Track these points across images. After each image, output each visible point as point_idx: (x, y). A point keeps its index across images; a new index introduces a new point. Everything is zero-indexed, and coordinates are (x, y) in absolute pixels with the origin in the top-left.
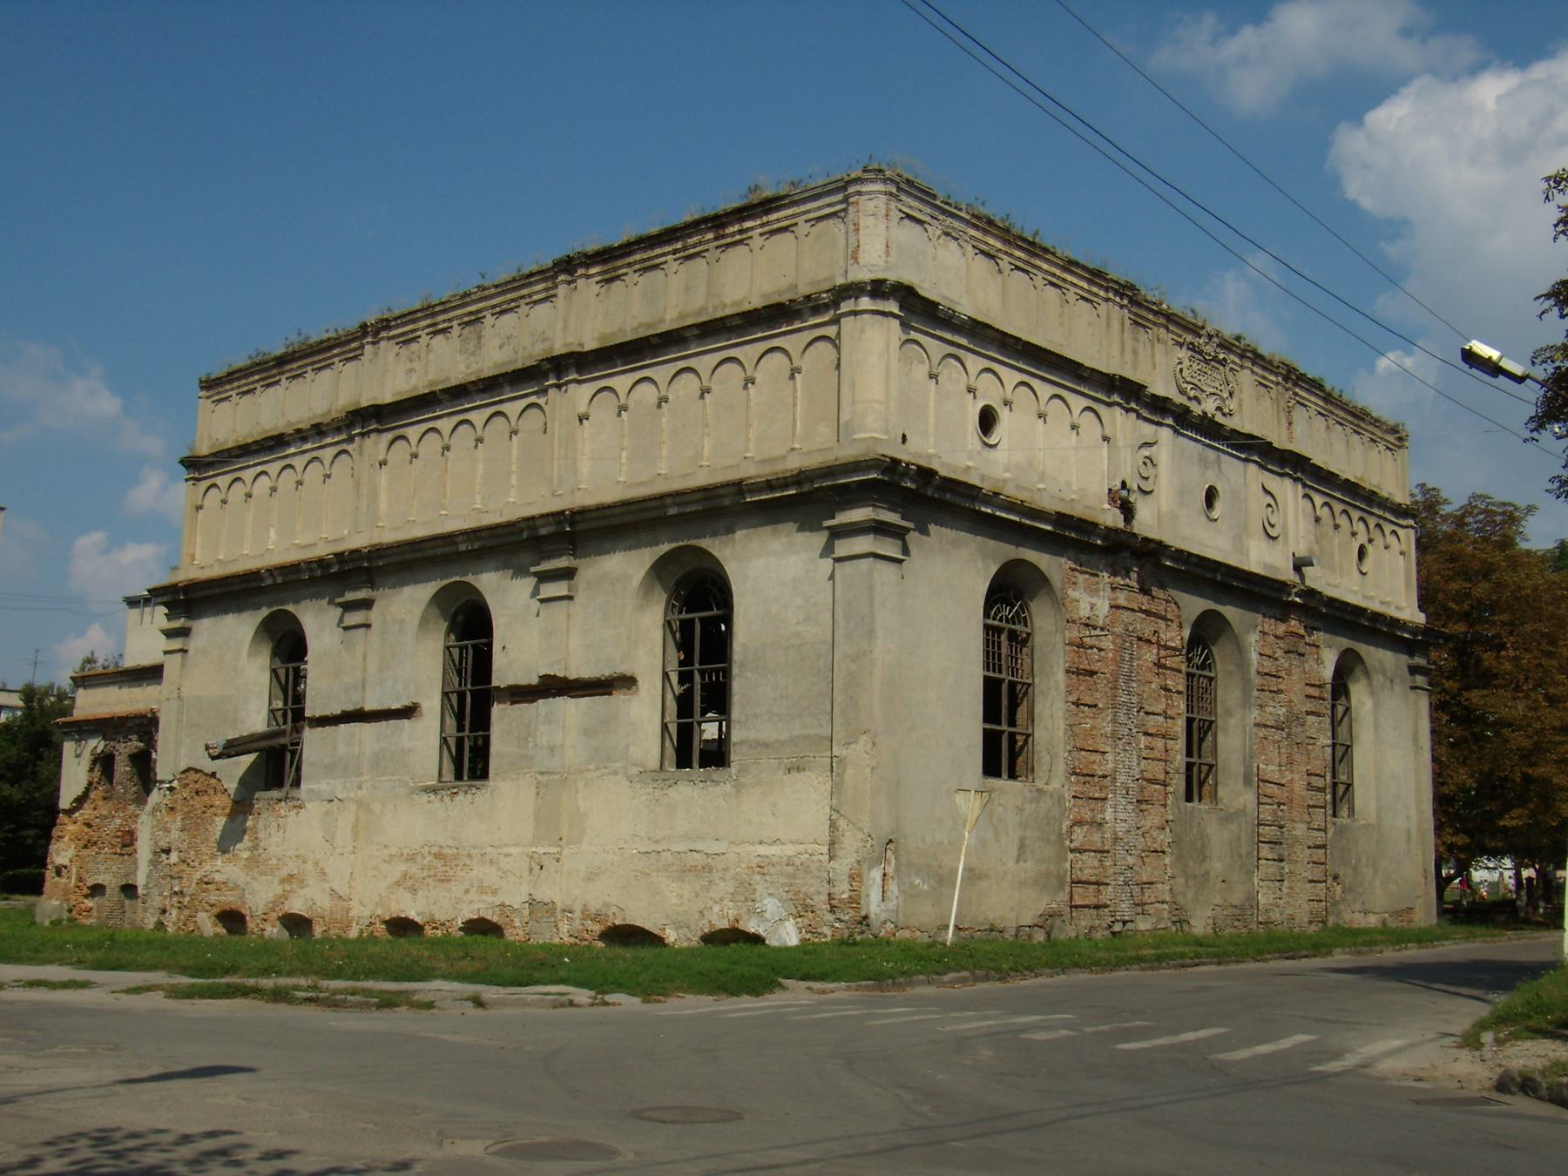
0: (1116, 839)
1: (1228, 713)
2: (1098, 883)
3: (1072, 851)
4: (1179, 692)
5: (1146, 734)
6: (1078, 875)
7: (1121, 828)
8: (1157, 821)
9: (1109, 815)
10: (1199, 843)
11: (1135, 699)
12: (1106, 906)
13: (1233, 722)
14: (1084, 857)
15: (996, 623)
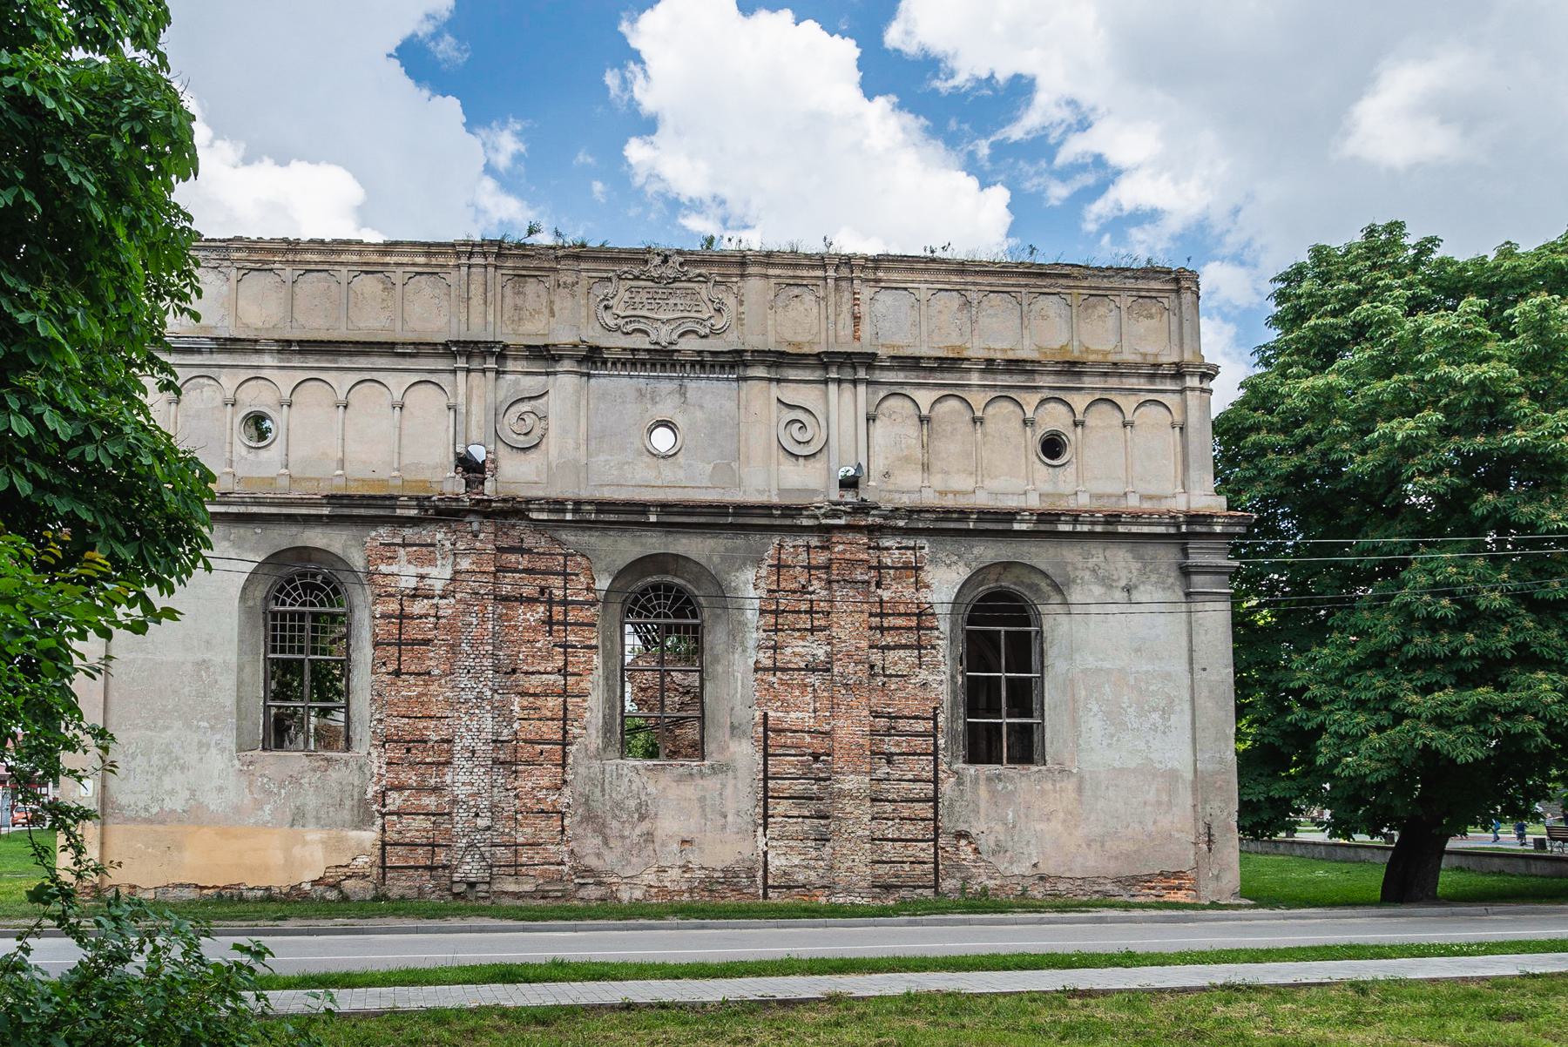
0: (454, 802)
1: (716, 660)
2: (434, 845)
3: (383, 815)
4: (590, 647)
5: (523, 694)
6: (392, 836)
7: (462, 792)
8: (545, 782)
9: (448, 779)
10: (632, 804)
11: (487, 662)
12: (444, 867)
13: (720, 669)
14: (406, 820)
15: (296, 608)
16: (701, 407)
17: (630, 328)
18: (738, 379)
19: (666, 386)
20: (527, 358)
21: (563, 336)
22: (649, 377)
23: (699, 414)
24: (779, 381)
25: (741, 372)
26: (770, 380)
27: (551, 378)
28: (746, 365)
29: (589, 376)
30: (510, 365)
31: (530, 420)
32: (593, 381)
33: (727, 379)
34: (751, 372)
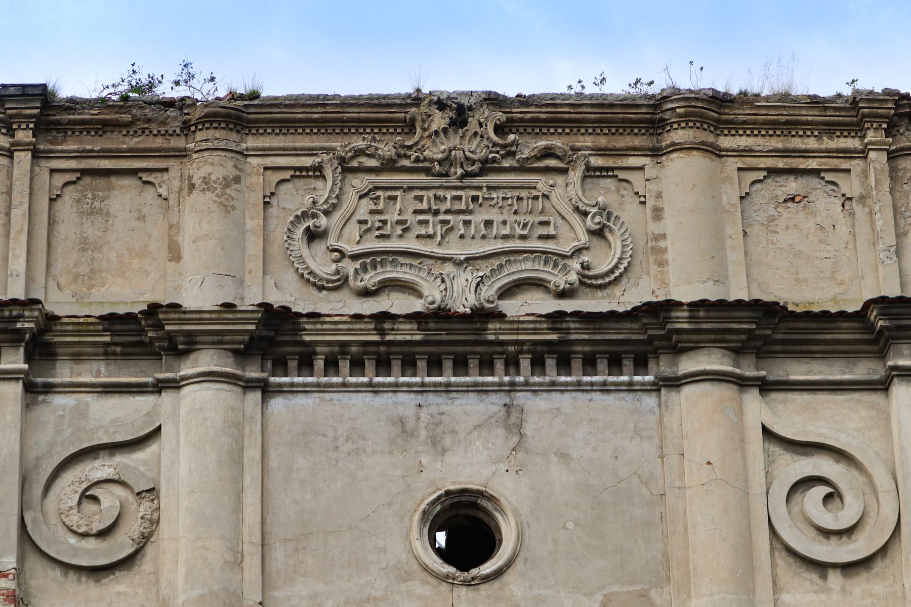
16: (564, 456)
17: (371, 279)
18: (656, 387)
19: (468, 409)
20: (107, 353)
21: (198, 293)
22: (423, 389)
23: (557, 473)
24: (766, 387)
25: (663, 367)
26: (742, 383)
27: (167, 397)
28: (678, 347)
29: (267, 390)
30: (64, 373)
31: (110, 498)
32: (278, 404)
33: (630, 388)
34: (688, 365)
